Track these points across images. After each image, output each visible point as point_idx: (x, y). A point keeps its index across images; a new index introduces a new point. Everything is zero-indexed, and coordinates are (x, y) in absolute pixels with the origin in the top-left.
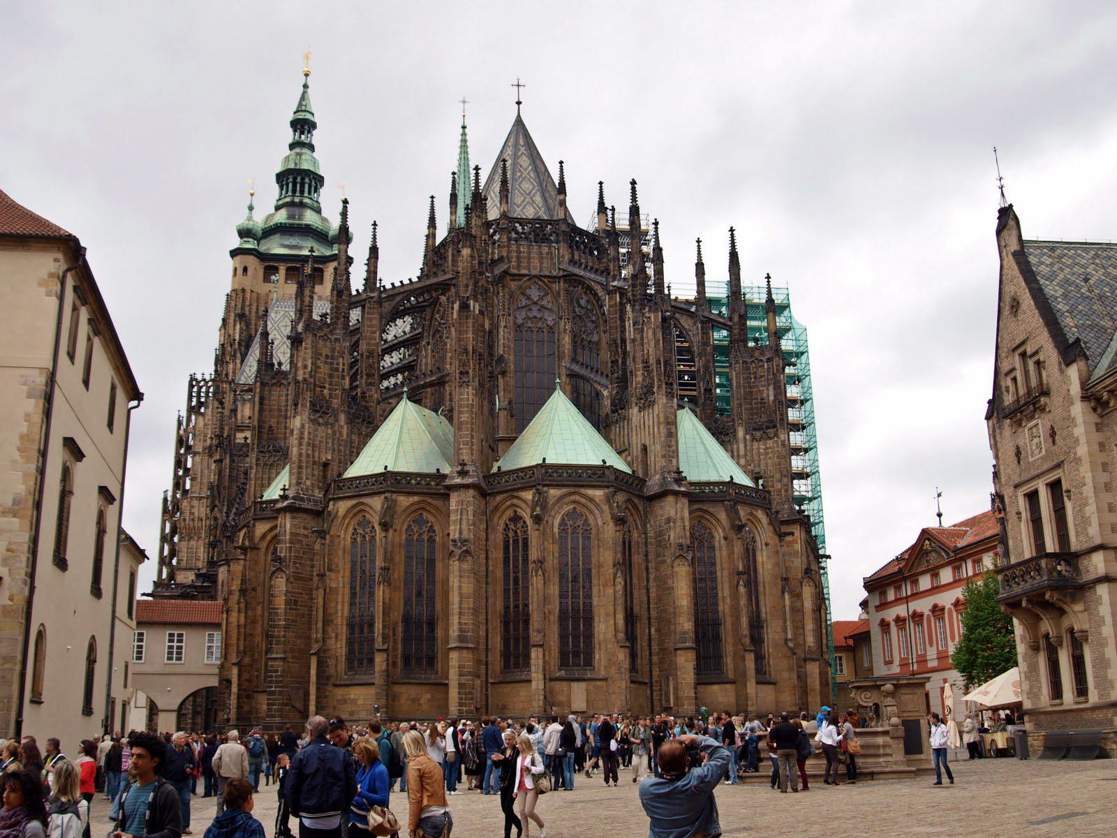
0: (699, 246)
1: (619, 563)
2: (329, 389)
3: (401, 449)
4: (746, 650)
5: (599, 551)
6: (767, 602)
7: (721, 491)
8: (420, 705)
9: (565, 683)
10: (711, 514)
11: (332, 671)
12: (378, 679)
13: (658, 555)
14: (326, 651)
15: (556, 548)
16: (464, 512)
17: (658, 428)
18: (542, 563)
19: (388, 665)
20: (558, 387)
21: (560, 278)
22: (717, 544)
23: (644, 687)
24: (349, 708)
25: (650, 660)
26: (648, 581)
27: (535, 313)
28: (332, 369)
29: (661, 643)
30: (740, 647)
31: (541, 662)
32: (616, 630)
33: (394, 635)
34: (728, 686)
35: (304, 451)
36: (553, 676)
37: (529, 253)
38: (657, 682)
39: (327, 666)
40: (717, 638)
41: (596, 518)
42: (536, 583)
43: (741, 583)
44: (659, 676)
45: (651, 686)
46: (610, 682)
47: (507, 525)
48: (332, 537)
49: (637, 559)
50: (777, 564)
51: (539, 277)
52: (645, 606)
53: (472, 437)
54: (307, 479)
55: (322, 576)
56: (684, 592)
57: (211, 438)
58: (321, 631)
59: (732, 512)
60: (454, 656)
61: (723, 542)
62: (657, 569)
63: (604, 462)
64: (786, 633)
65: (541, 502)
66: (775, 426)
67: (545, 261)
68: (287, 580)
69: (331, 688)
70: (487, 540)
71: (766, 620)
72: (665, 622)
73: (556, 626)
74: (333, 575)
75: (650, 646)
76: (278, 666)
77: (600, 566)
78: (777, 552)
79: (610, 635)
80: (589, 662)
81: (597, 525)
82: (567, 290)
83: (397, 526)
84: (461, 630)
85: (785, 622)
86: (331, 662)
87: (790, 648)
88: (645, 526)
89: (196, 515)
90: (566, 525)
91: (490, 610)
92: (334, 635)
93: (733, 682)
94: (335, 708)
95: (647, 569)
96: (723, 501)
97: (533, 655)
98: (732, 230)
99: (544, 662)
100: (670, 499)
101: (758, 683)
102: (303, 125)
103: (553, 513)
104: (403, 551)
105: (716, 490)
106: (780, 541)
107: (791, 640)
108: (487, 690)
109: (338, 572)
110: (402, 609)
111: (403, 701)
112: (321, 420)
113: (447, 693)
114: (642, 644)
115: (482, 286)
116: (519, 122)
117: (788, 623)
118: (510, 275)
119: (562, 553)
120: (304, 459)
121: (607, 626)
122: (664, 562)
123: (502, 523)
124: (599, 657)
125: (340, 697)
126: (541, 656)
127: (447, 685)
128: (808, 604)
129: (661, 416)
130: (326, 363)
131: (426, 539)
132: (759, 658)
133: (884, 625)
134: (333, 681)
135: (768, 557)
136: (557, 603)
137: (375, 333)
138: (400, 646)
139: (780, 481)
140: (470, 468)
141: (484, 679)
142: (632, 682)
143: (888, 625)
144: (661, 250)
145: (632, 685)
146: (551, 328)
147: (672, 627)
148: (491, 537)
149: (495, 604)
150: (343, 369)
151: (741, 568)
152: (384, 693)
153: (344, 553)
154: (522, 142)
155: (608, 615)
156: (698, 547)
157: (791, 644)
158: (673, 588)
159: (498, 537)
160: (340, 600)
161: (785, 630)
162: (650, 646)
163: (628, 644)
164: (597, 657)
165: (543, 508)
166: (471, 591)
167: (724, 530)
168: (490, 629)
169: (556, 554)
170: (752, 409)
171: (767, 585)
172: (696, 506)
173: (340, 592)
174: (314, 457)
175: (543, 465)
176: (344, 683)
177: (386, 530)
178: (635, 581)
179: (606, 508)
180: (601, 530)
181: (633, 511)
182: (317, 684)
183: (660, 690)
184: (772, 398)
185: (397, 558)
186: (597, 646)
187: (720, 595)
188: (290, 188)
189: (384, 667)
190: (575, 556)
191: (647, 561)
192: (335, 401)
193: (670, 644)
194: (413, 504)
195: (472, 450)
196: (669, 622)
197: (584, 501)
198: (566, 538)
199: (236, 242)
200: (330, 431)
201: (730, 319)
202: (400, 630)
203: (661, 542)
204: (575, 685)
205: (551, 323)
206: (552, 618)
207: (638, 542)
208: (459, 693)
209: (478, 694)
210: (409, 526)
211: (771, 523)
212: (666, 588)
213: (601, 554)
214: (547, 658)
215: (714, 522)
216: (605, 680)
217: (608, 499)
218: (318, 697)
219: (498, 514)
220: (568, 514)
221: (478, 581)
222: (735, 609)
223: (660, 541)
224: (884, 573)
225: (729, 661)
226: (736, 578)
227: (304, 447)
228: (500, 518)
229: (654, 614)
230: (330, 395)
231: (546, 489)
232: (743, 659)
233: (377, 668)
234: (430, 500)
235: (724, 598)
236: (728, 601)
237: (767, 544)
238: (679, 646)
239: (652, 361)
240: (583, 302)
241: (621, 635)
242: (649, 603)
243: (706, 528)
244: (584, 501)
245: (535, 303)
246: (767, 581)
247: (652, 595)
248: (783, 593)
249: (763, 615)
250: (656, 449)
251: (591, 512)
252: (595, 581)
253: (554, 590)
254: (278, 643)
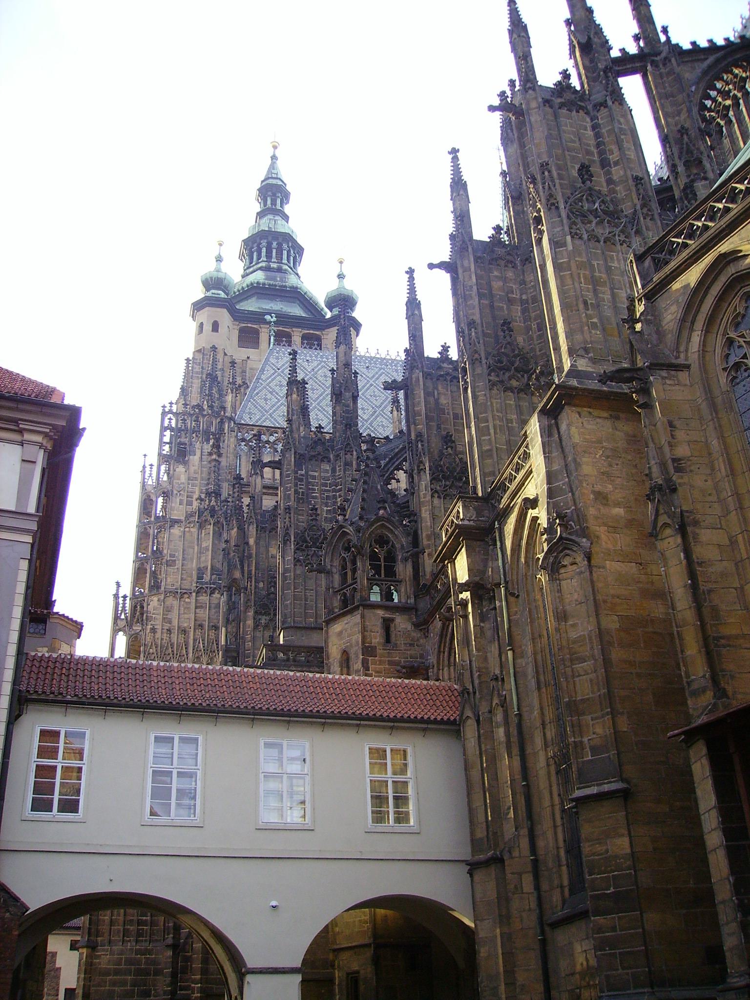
57: (200, 499)
89: (175, 623)
102: (273, 194)
188: (264, 253)
199: (199, 293)
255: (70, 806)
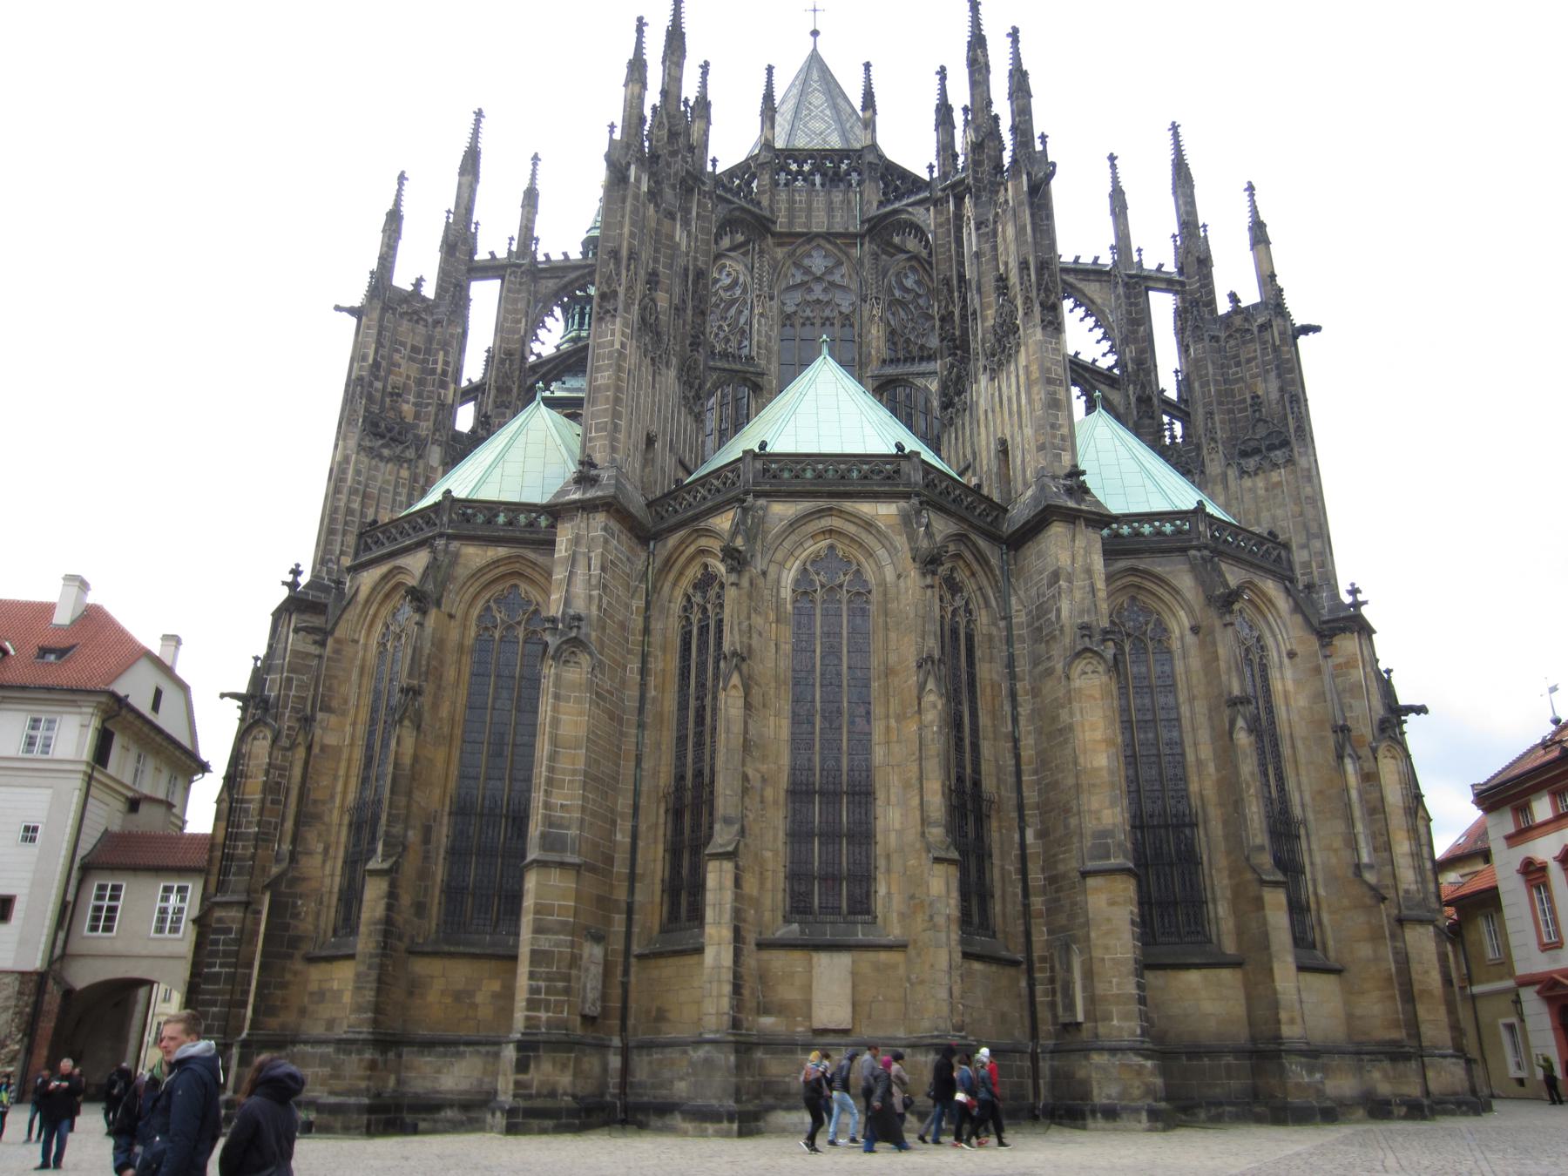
0: (1113, 167)
1: (930, 657)
2: (415, 404)
3: (498, 471)
4: (1263, 883)
5: (887, 640)
6: (1304, 780)
7: (1178, 532)
8: (474, 1006)
9: (797, 956)
10: (1160, 580)
11: (306, 926)
12: (365, 942)
13: (1036, 662)
14: (295, 881)
15: (787, 633)
16: (582, 562)
17: (1028, 393)
18: (743, 659)
19: (389, 907)
20: (825, 350)
21: (862, 236)
22: (1176, 645)
23: (1012, 971)
24: (326, 1011)
25: (1026, 906)
26: (1015, 721)
27: (818, 292)
28: (424, 371)
29: (1050, 861)
30: (1249, 876)
31: (728, 896)
32: (924, 821)
33: (426, 840)
34: (1226, 974)
35: (342, 504)
36: (768, 935)
37: (809, 203)
38: (1043, 959)
39: (296, 916)
40: (1189, 859)
41: (880, 567)
42: (730, 703)
43: (1240, 723)
44: (1049, 945)
45: (1030, 972)
46: (912, 951)
47: (689, 600)
48: (338, 641)
49: (989, 672)
50: (1320, 696)
51: (829, 236)
52: (1011, 780)
53: (616, 415)
54: (342, 553)
55: (307, 721)
56: (1098, 735)
58: (288, 838)
59: (1206, 574)
60: (531, 882)
61: (1190, 638)
62: (1035, 692)
63: (900, 447)
64: (1356, 850)
65: (751, 528)
66: (1285, 443)
67: (838, 214)
68: (274, 741)
69: (299, 965)
70: (646, 631)
71: (1305, 822)
72: (1056, 811)
73: (781, 814)
74: (333, 719)
75: (1024, 872)
76: (233, 920)
77: (889, 672)
78: (1317, 670)
79: (912, 835)
80: (862, 906)
81: (883, 583)
82: (876, 256)
83: (455, 601)
84: (549, 821)
85: (1350, 823)
86: (306, 907)
87: (1372, 888)
88: (1007, 603)
90: (812, 582)
91: (645, 788)
92: (320, 847)
93: (1236, 964)
94: (303, 1012)
95: (1013, 695)
96: (1183, 550)
97: (711, 880)
98: (1175, 128)
99: (738, 897)
100: (1057, 530)
101: (1301, 968)
103: (779, 556)
104: (466, 660)
105: (1168, 528)
106: (1323, 646)
107: (1370, 867)
108: (626, 972)
109: (344, 713)
110: (452, 785)
111: (432, 997)
112: (386, 452)
113: (513, 973)
114: (1002, 867)
115: (676, 174)
116: (815, 60)
117: (1359, 827)
118: (774, 235)
119: (802, 648)
120: (340, 517)
121: (906, 813)
122: (1049, 672)
123: (679, 595)
124: (888, 892)
125: (313, 987)
126: (729, 882)
127: (514, 958)
128: (1394, 795)
129: (1034, 367)
130: (411, 359)
131: (521, 636)
132: (1297, 909)
133: (1533, 873)
134: (307, 948)
135: (1296, 682)
136: (785, 760)
137: (519, 321)
138: (439, 872)
139: (1305, 546)
140: (605, 476)
141: (619, 946)
142: (966, 955)
143: (1543, 868)
144: (1024, 75)
145: (977, 966)
146: (847, 317)
147: (1073, 821)
148: (657, 626)
149: (656, 773)
150: (444, 373)
151: (1236, 692)
152: (374, 974)
153: (361, 674)
154: (815, 76)
155: (906, 785)
156: (1127, 643)
157: (1370, 877)
158: (1070, 728)
159: (668, 627)
160: (342, 772)
161: (1352, 843)
162: (1024, 872)
163: (955, 855)
164: (882, 890)
165: (750, 539)
166: (582, 733)
167: (1190, 612)
168: (643, 827)
169: (787, 648)
170: (1234, 421)
171: (1299, 744)
172: (1122, 564)
173: (345, 756)
174: (363, 515)
175: (761, 455)
176: (324, 953)
177: (424, 612)
178: (984, 720)
179: (901, 541)
180: (892, 592)
181: (976, 566)
182: (264, 954)
183: (1052, 980)
184: (1274, 395)
185: (450, 674)
186: (881, 863)
187: (1190, 757)
189: (380, 911)
190: (832, 652)
191: (1013, 677)
192: (423, 424)
193: (1070, 864)
194: (496, 563)
195: (613, 439)
196: (1067, 811)
197: (851, 529)
198: (811, 616)
200: (405, 473)
201: (1181, 271)
202: (444, 830)
203: (1042, 628)
204: (823, 960)
205: (846, 309)
206: (769, 793)
207: (990, 638)
208: (532, 976)
209: (590, 982)
210: (488, 609)
211: (1297, 608)
212: (1056, 733)
213: (893, 645)
214: (750, 886)
215: (1167, 597)
216: (901, 947)
217: (906, 520)
218: (260, 986)
219: (671, 576)
220: (816, 560)
221: (615, 718)
222: (1230, 788)
223: (1040, 629)
224: (1529, 765)
225: (1222, 913)
226: (1227, 712)
227: (343, 497)
228: (675, 584)
229: (1031, 796)
230: (417, 416)
231: (762, 502)
232: (1259, 903)
233: (365, 916)
234: (531, 555)
235: (1199, 762)
236: (1211, 768)
237: (1292, 655)
238: (1091, 865)
239: (1014, 279)
240: (909, 283)
241: (937, 833)
242: (1018, 773)
243: (1147, 611)
244: (851, 529)
245: (818, 279)
246: (1301, 730)
247: (1027, 753)
248: (1340, 758)
249: (1297, 811)
250: (1024, 439)
251: (870, 554)
252: (877, 710)
253: (777, 727)
254: (239, 872)
255: (108, 929)
